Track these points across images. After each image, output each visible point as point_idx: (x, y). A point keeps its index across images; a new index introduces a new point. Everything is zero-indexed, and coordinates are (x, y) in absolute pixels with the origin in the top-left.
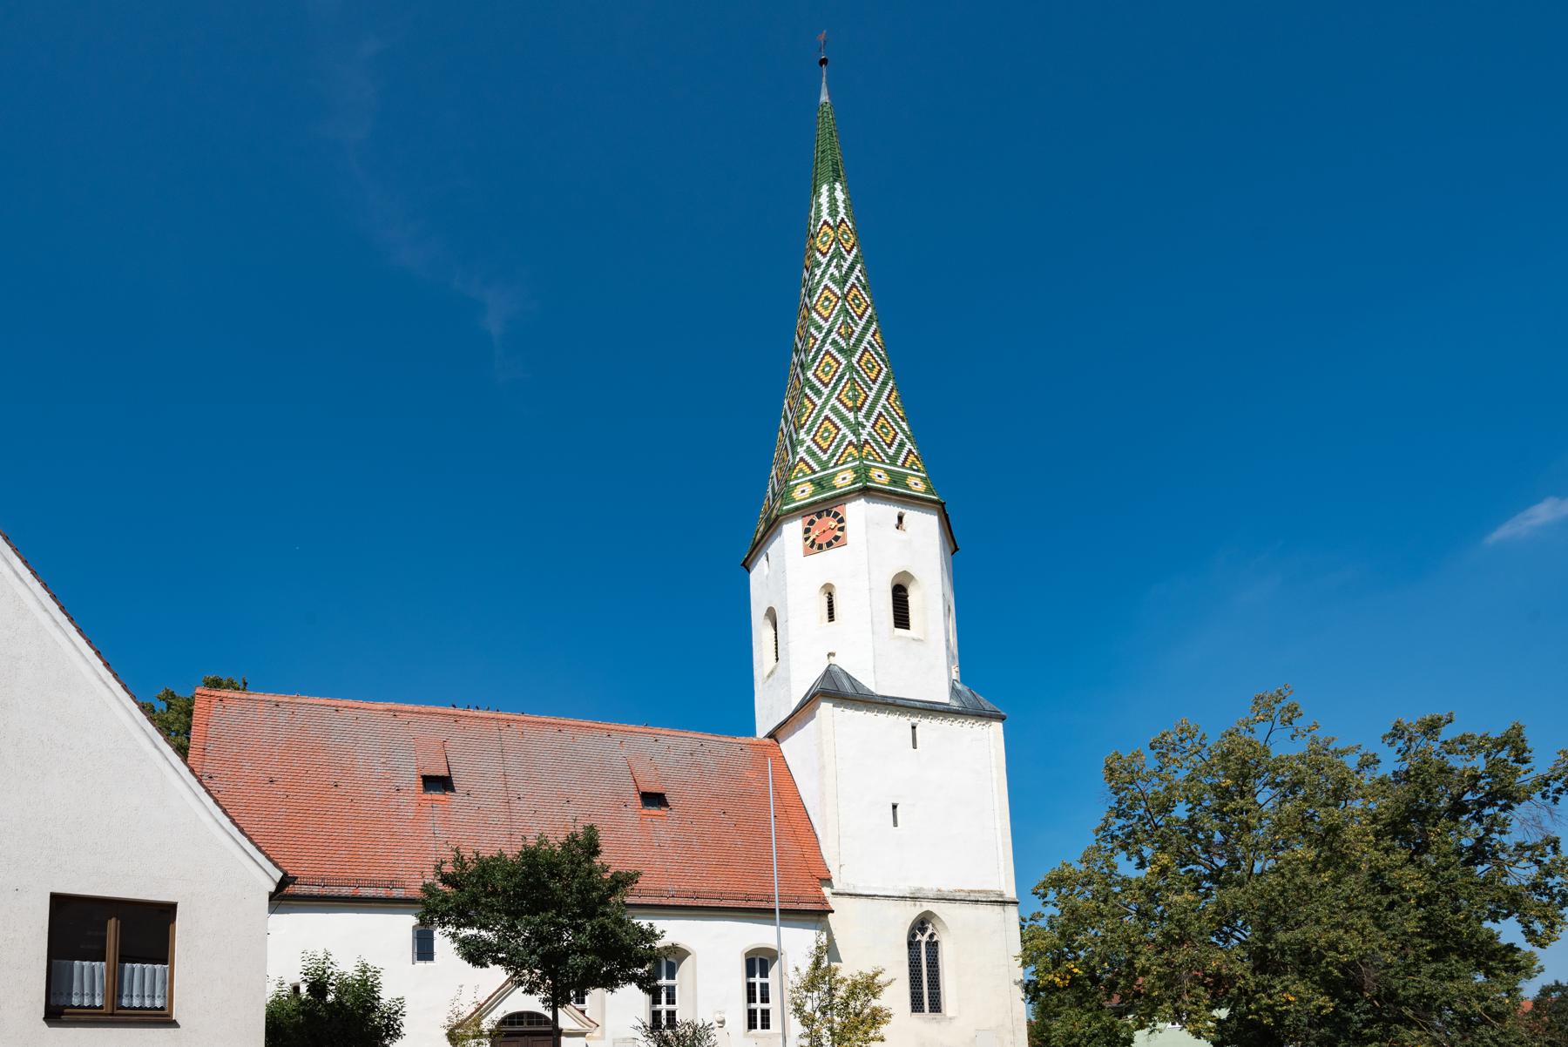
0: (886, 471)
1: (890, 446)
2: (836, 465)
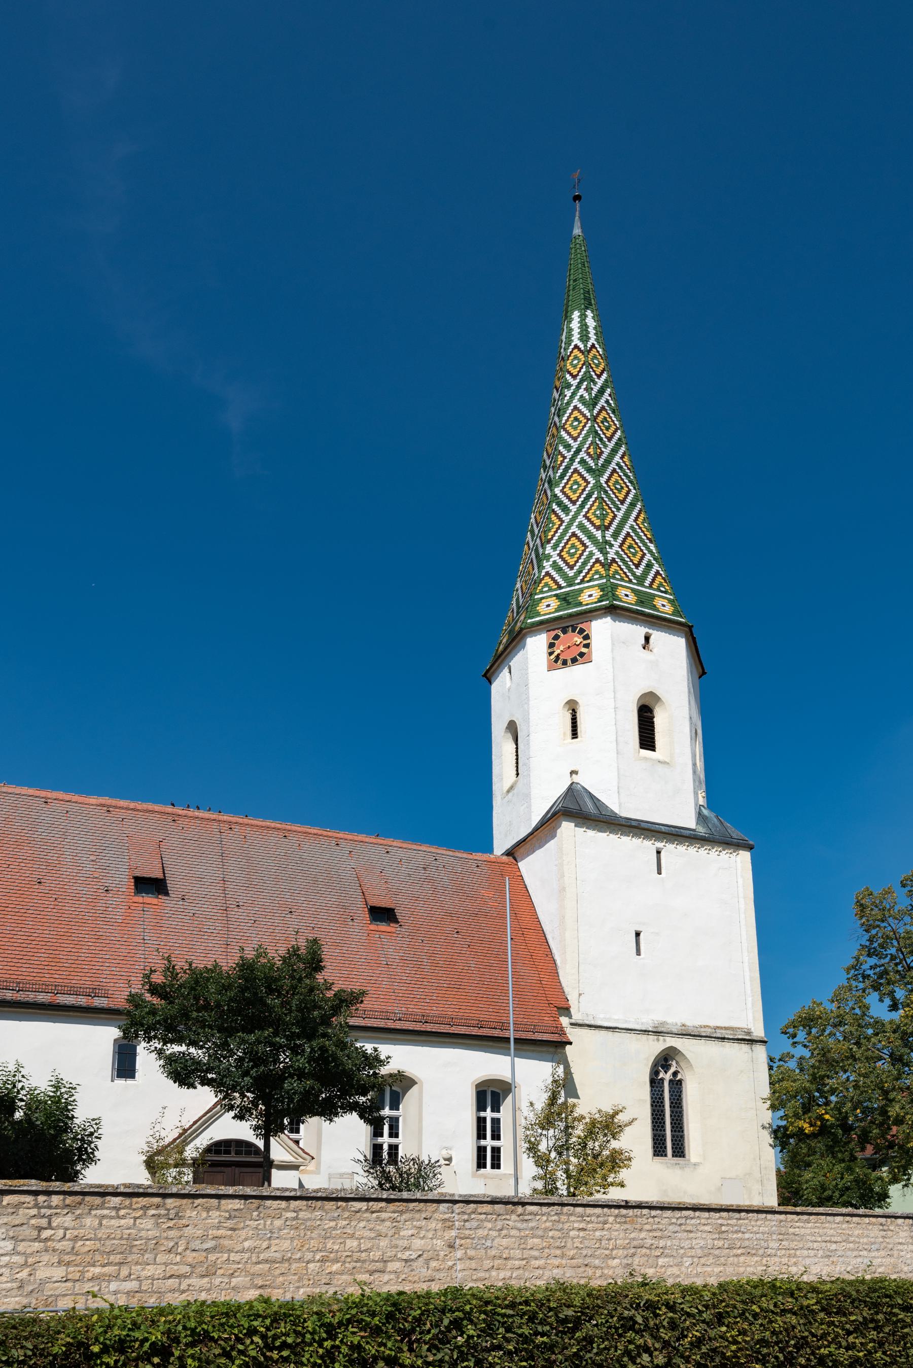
0: (633, 590)
1: (637, 566)
2: (582, 581)
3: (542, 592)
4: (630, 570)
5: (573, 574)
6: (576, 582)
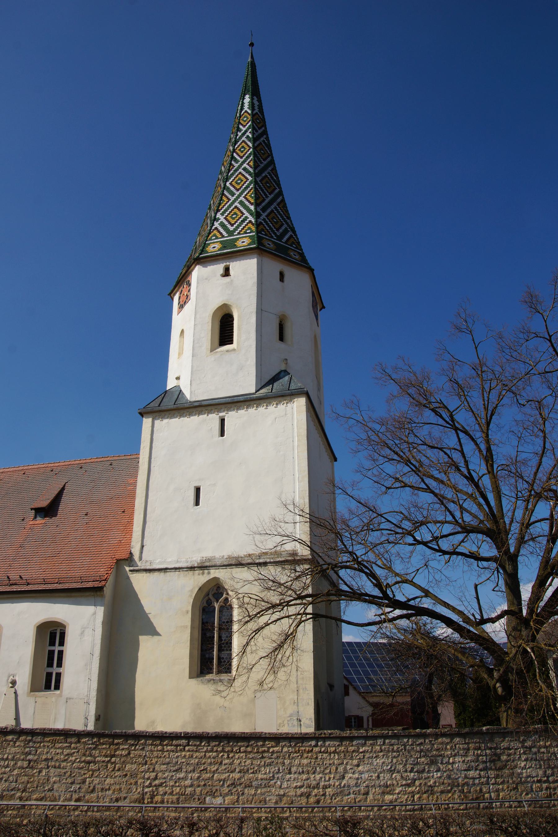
0: (273, 242)
1: (278, 230)
2: (239, 234)
3: (211, 239)
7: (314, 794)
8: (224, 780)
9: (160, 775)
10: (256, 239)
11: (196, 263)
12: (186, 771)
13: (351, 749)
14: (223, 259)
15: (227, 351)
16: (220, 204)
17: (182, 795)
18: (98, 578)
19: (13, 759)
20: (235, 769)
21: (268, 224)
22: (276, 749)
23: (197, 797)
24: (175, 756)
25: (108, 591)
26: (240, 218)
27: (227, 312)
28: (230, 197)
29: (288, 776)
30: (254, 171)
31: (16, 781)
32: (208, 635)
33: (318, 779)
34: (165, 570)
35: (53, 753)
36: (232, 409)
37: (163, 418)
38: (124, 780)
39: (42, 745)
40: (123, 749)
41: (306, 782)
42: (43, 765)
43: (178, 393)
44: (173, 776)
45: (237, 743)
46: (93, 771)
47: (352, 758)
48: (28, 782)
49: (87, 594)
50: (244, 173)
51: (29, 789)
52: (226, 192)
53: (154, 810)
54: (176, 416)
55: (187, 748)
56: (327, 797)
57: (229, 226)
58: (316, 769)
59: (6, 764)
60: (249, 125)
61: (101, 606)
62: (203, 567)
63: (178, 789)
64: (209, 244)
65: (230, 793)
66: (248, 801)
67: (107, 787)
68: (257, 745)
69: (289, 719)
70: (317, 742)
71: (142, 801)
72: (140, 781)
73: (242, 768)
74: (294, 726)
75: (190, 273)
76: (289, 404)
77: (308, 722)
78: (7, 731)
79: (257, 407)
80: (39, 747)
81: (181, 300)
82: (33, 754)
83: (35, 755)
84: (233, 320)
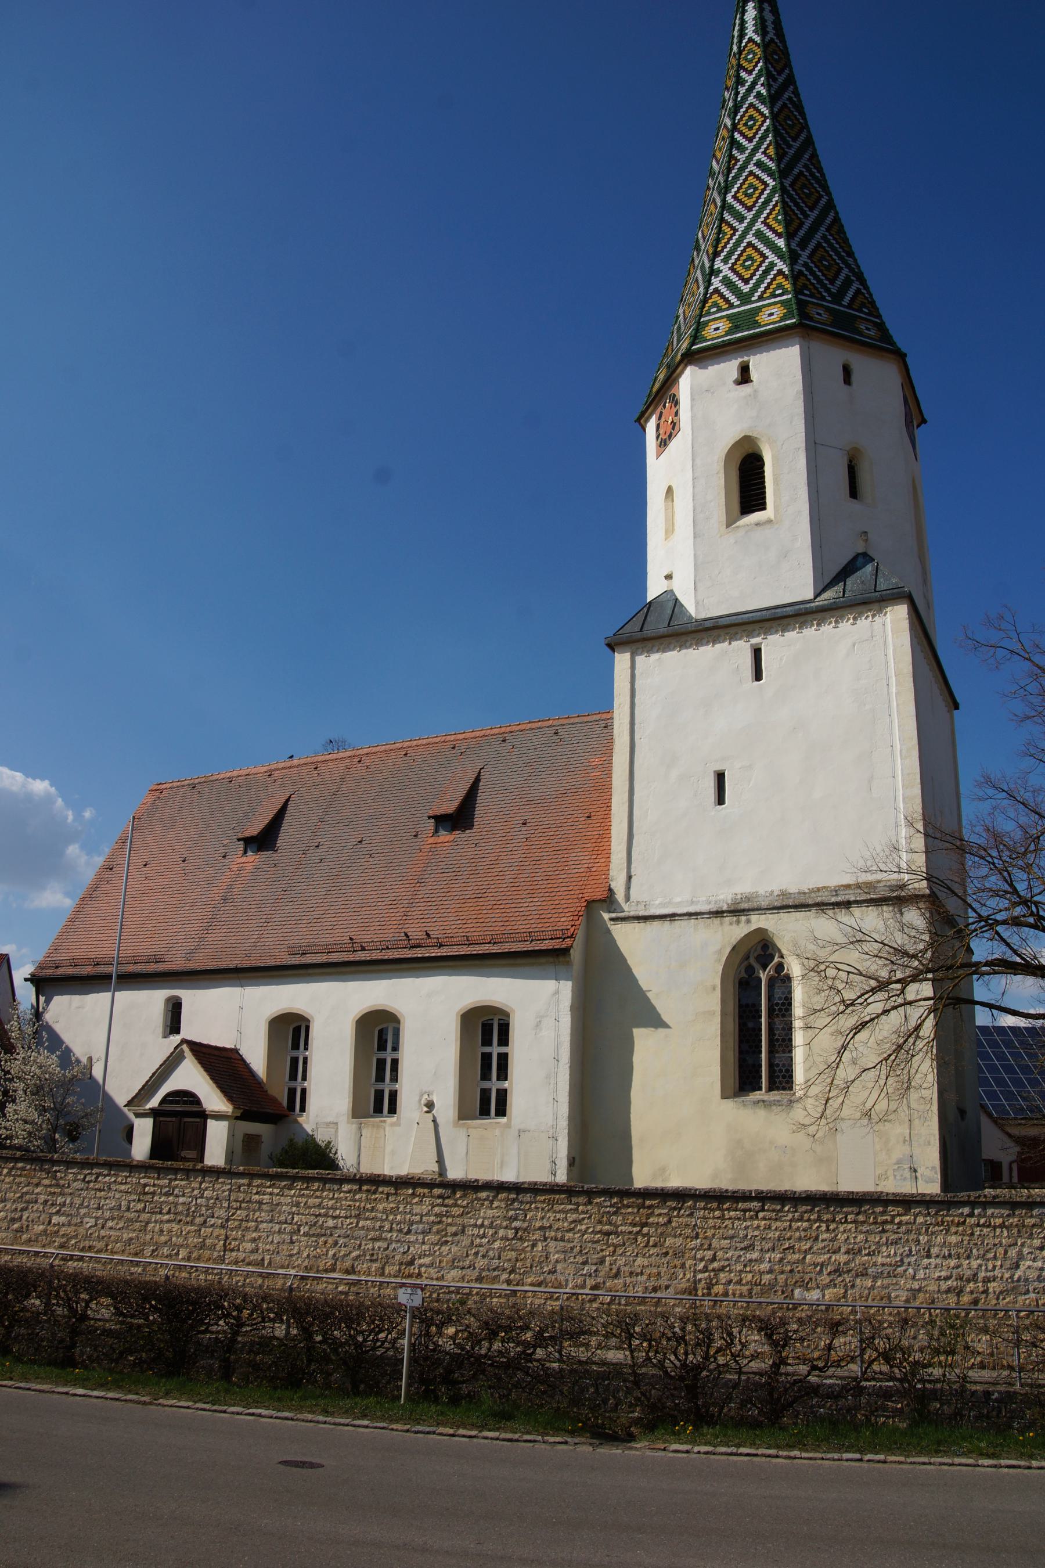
0: (827, 309)
1: (832, 283)
2: (761, 298)
3: (709, 313)
4: (824, 286)
5: (748, 290)
6: (753, 299)
7: (968, 1289)
8: (822, 1265)
9: (720, 1254)
10: (794, 307)
11: (686, 361)
12: (762, 1250)
13: (1030, 1221)
14: (736, 350)
15: (757, 524)
16: (718, 241)
17: (757, 1286)
18: (558, 934)
19: (491, 1226)
20: (840, 1247)
21: (812, 273)
22: (904, 1218)
23: (780, 1289)
24: (743, 1226)
25: (576, 954)
26: (760, 265)
27: (751, 451)
28: (736, 224)
29: (926, 1261)
30: (778, 166)
31: (499, 1258)
32: (750, 1025)
33: (975, 1267)
34: (672, 917)
35: (552, 1218)
36: (773, 630)
37: (650, 651)
38: (665, 1260)
39: (533, 1206)
40: (660, 1215)
41: (954, 1271)
42: (537, 1236)
43: (671, 604)
44: (740, 1256)
45: (842, 1208)
46: (616, 1246)
47: (1031, 1236)
48: (517, 1260)
49: (543, 960)
50: (758, 172)
51: (520, 1269)
52: (727, 216)
53: (714, 1305)
54: (672, 646)
55: (761, 1215)
56: (991, 1296)
57: (740, 284)
58: (971, 1251)
59: (481, 1232)
60: (758, 68)
61: (567, 979)
62: (737, 911)
63: (750, 1276)
64: (707, 323)
65: (832, 1284)
66: (861, 1297)
67: (639, 1271)
68: (874, 1212)
69: (896, 1167)
70: (973, 1209)
71: (694, 1292)
72: (689, 1263)
73: (851, 1247)
74: (905, 1179)
75: (676, 380)
76: (876, 618)
77: (928, 1173)
78: (478, 1186)
79: (819, 625)
80: (530, 1209)
81: (662, 431)
82: (520, 1220)
83: (524, 1221)
84: (763, 464)
